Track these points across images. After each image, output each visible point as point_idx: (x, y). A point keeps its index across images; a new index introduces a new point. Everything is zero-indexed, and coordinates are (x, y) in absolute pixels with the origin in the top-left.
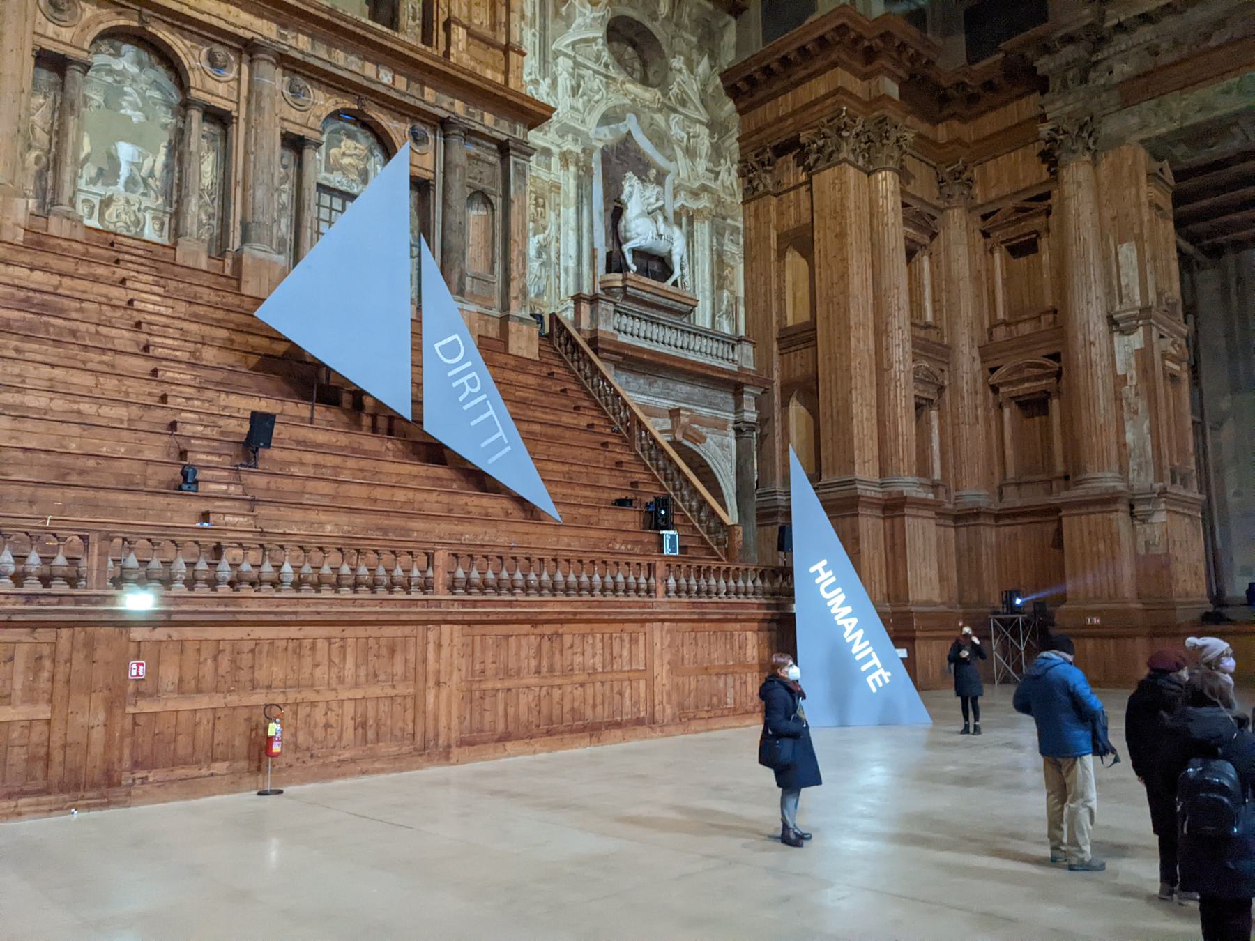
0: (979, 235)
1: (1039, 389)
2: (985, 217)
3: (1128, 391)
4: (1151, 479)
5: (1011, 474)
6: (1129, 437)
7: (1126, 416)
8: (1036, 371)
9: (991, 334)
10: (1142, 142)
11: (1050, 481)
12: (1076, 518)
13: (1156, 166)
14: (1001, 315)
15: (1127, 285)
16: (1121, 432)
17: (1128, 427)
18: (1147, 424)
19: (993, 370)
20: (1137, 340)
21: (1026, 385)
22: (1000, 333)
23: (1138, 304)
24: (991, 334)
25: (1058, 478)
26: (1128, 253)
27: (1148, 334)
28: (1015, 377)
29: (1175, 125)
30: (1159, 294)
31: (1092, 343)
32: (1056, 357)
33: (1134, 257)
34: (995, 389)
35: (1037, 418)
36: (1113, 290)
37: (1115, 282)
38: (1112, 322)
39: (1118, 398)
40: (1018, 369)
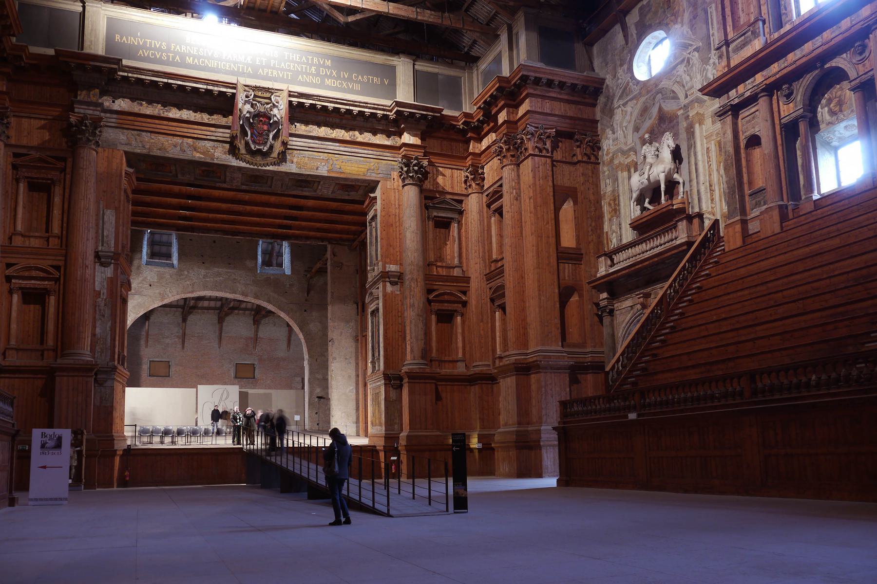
0: (10, 167)
1: (41, 287)
2: (16, 155)
3: (101, 301)
4: (108, 359)
5: (13, 342)
6: (98, 330)
7: (97, 317)
8: (42, 274)
9: (10, 238)
10: (126, 153)
11: (43, 351)
12: (65, 378)
13: (131, 170)
14: (19, 228)
15: (107, 236)
16: (94, 327)
17: (98, 324)
18: (109, 324)
19: (9, 265)
20: (109, 272)
21: (33, 282)
22: (18, 241)
23: (113, 250)
24: (10, 238)
25: (48, 350)
26: (110, 216)
27: (116, 270)
28: (26, 274)
29: (145, 151)
30: (123, 247)
31: (87, 266)
32: (57, 268)
33: (113, 219)
34: (8, 279)
35: (32, 306)
36: (100, 237)
37: (100, 231)
38: (97, 256)
39: (95, 306)
40: (29, 268)
